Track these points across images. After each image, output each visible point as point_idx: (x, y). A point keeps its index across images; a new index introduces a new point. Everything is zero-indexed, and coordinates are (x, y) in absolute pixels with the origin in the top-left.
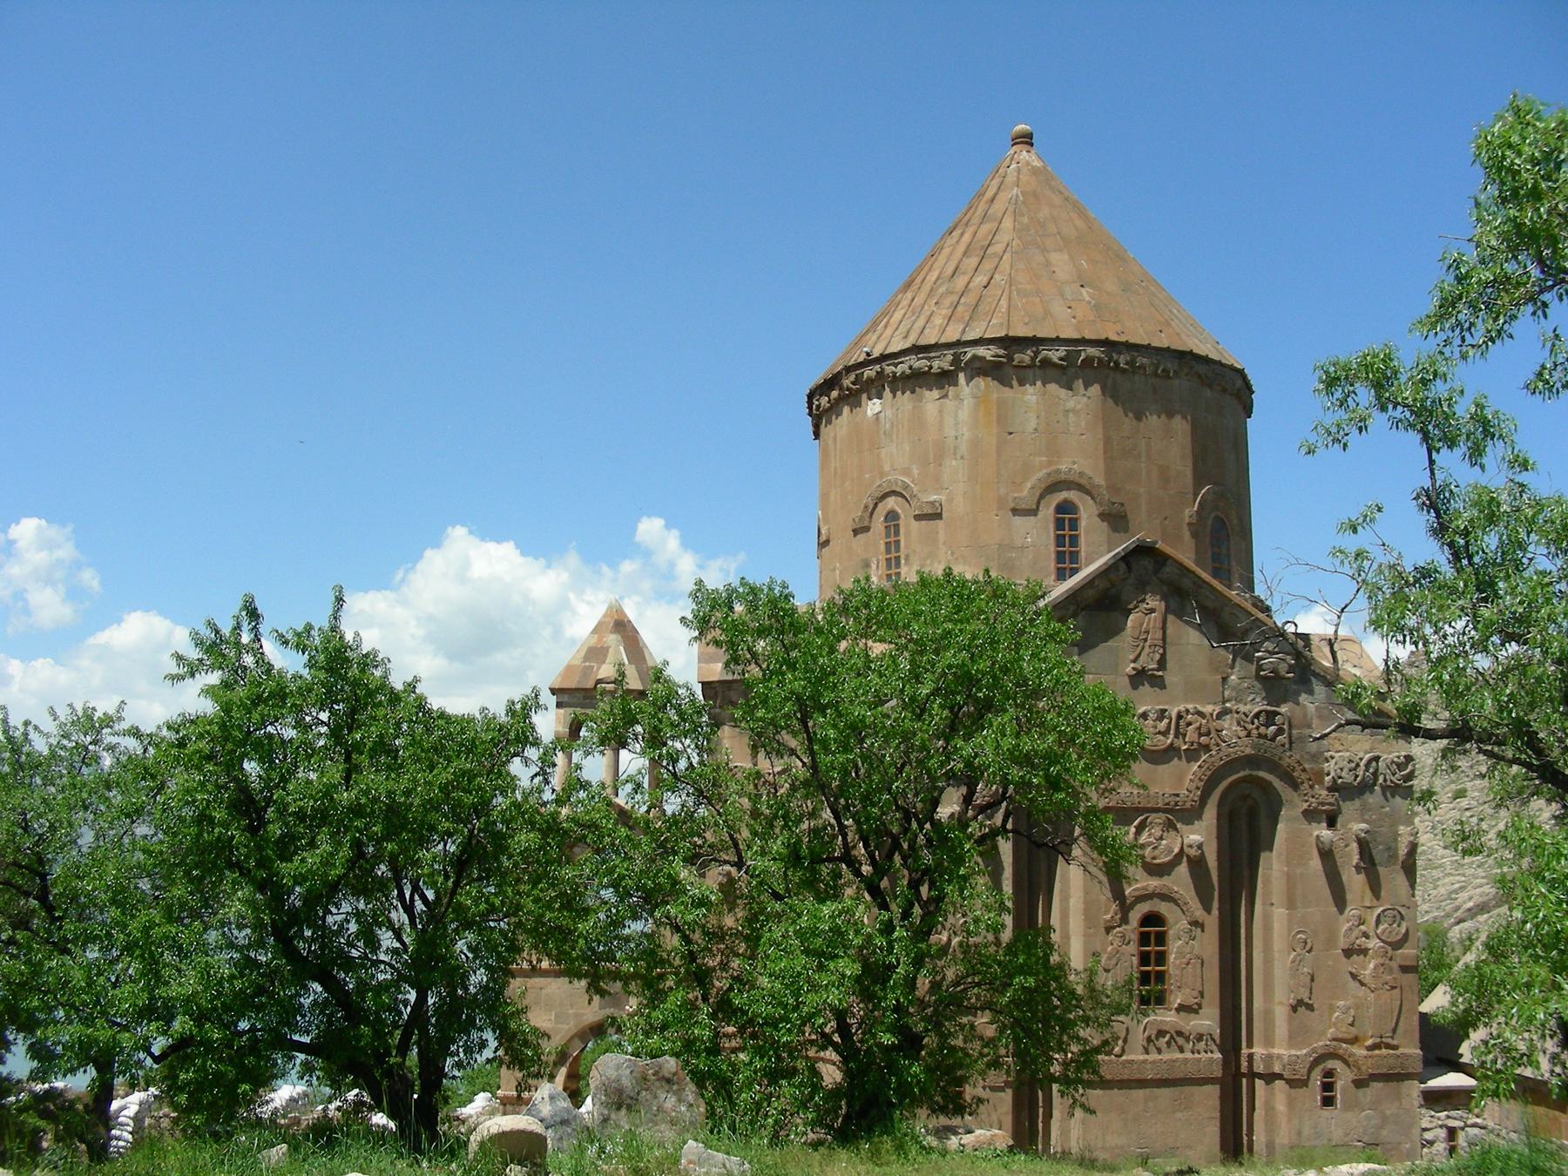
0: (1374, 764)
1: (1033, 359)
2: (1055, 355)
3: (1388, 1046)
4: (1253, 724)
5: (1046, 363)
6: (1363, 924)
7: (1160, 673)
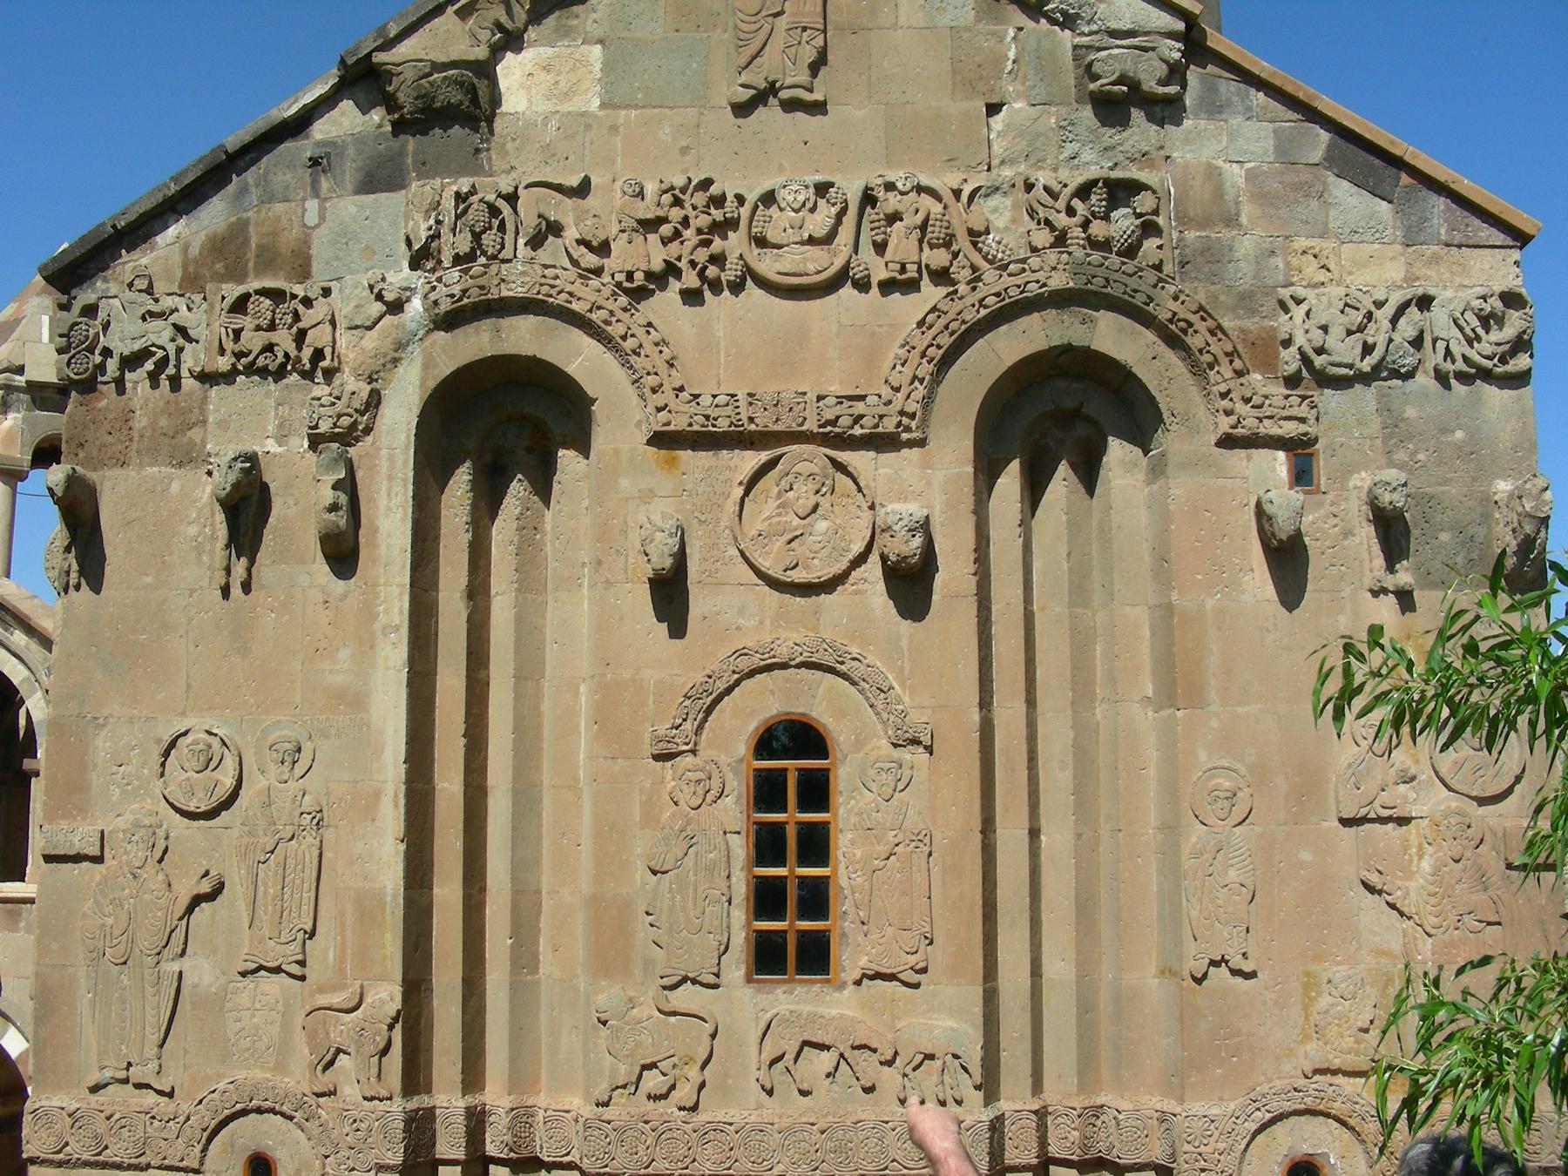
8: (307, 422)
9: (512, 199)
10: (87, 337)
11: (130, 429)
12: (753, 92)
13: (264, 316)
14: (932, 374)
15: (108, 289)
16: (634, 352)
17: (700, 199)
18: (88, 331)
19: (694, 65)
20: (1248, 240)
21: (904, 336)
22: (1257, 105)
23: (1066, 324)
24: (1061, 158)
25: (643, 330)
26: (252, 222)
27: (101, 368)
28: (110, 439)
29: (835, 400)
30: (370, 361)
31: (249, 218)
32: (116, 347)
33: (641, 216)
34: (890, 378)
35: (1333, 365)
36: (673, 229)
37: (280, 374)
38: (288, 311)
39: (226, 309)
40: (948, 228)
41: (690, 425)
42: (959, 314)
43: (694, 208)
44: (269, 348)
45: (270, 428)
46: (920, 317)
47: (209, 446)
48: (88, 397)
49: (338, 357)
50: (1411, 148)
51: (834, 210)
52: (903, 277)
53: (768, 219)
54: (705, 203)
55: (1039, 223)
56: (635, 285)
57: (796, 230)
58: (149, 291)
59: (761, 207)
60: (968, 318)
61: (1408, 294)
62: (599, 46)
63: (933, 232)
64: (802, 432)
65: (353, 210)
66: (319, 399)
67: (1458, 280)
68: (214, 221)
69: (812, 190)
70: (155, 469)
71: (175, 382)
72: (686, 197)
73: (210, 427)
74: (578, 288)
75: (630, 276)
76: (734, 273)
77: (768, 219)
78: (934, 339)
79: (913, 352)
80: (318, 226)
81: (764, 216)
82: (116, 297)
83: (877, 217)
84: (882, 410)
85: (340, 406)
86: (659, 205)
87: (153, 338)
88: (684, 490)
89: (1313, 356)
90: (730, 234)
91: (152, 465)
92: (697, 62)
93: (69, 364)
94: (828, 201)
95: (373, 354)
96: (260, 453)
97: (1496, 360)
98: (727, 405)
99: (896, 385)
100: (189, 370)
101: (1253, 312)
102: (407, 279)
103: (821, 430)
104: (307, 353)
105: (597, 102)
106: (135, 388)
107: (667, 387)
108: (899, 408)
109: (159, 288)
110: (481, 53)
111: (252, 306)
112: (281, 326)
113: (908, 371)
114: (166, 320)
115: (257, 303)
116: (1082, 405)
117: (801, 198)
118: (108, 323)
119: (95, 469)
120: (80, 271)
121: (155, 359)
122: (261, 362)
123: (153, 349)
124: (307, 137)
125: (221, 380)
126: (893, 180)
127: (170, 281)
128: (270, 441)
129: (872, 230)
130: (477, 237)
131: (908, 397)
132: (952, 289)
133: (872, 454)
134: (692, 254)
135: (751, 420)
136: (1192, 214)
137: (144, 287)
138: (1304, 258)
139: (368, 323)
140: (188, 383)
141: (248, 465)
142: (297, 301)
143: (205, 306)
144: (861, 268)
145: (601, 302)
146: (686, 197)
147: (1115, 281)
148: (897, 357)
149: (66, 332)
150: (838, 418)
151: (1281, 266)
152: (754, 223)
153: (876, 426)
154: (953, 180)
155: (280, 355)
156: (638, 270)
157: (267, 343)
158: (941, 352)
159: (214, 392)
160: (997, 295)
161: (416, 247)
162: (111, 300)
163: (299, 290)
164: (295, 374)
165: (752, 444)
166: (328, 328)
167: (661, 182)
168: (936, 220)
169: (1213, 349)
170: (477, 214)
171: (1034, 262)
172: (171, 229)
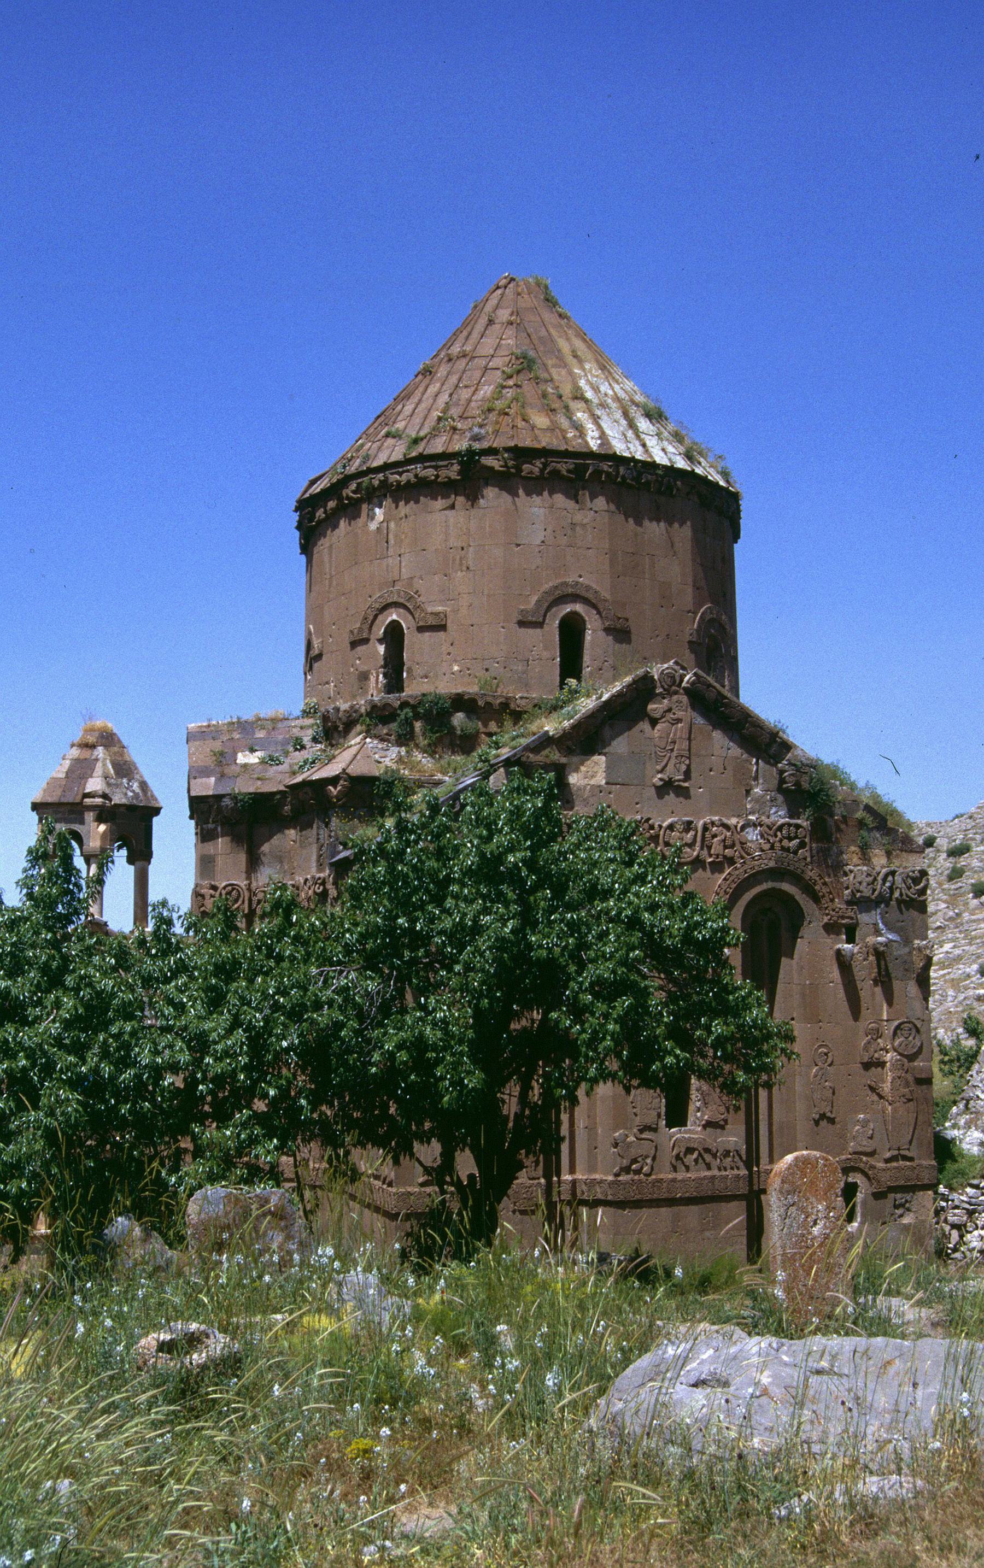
0: (890, 878)
1: (542, 471)
2: (563, 467)
3: (905, 1158)
4: (776, 836)
5: (556, 473)
6: (880, 1037)
7: (686, 785)
105: (604, 782)
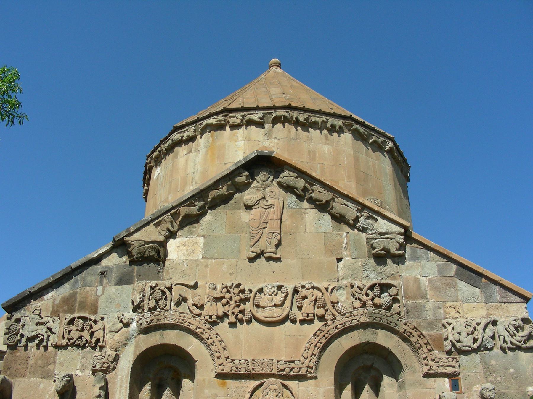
8: (92, 365)
9: (170, 289)
10: (16, 330)
11: (28, 364)
12: (256, 254)
13: (79, 326)
14: (319, 353)
15: (25, 313)
16: (211, 344)
17: (236, 290)
18: (16, 327)
19: (235, 245)
20: (430, 303)
21: (308, 339)
22: (431, 257)
23: (367, 335)
24: (363, 276)
25: (215, 336)
26: (78, 293)
27: (20, 341)
28: (20, 367)
29: (283, 362)
30: (116, 344)
31: (77, 292)
32: (26, 334)
33: (215, 296)
34: (304, 354)
35: (463, 346)
36: (226, 301)
37: (84, 347)
38: (88, 325)
39: (66, 323)
40: (324, 301)
41: (231, 371)
42: (328, 331)
43: (234, 294)
44: (81, 337)
45: (78, 366)
46: (314, 332)
47: (55, 372)
48: (14, 351)
49: (105, 342)
50: (485, 270)
51: (283, 295)
52: (308, 318)
53: (260, 298)
54: (238, 292)
55: (356, 299)
56: (212, 320)
57: (270, 302)
58: (40, 315)
59: (258, 294)
60: (331, 333)
61: (488, 320)
62: (202, 238)
63: (319, 303)
64: (272, 374)
65: (114, 290)
66: (97, 357)
67: (506, 315)
68: (65, 292)
69: (276, 288)
70: (35, 379)
71: (46, 348)
72: (231, 290)
73: (57, 365)
74: (192, 321)
75: (211, 317)
76: (248, 317)
77: (260, 298)
78: (319, 340)
79: (312, 345)
80: (101, 295)
81: (259, 297)
82: (28, 316)
83: (299, 297)
84: (301, 366)
85: (104, 360)
86: (222, 292)
87: (40, 332)
88: (228, 395)
89: (456, 343)
90: (247, 303)
91: (34, 377)
92: (236, 244)
93: (8, 339)
94: (281, 292)
95: (117, 341)
96: (74, 375)
97: (522, 342)
98: (245, 364)
99: (306, 357)
100: (51, 344)
101: (433, 329)
102: (131, 315)
103: (279, 373)
104: (94, 340)
105: (201, 257)
106: (31, 349)
107: (223, 357)
108: (307, 365)
109: (43, 314)
110: (162, 238)
111: (75, 322)
112: (85, 330)
113: (310, 352)
114: (45, 325)
115: (77, 321)
116: (373, 364)
117: (272, 291)
118: (24, 325)
119: (13, 378)
120: (16, 306)
121: (39, 339)
122: (77, 342)
123: (39, 335)
124: (100, 265)
125: (62, 348)
126: (304, 284)
127: (47, 312)
128: (78, 371)
129: (297, 302)
130: (157, 302)
131: (310, 361)
132: (325, 322)
133: (297, 382)
134: (233, 310)
135: (253, 369)
136: (410, 295)
137: (38, 313)
138: (450, 309)
139: (116, 330)
140: (50, 348)
141: (69, 379)
142: (92, 321)
143: (59, 321)
144: (293, 315)
145: (200, 326)
146: (231, 290)
147: (384, 319)
148: (306, 347)
149: (8, 327)
150: (285, 369)
151: (442, 312)
152: (255, 299)
153: (299, 372)
154: (326, 284)
155: (84, 340)
156: (213, 315)
157: (80, 335)
158: (322, 345)
159: (59, 352)
160: (342, 324)
161: (135, 304)
162: (26, 317)
163: (93, 318)
164: (89, 347)
165: (253, 378)
166: (102, 331)
167: (223, 284)
168: (320, 298)
169: (420, 342)
170: (157, 294)
171: (355, 313)
172: (50, 294)
